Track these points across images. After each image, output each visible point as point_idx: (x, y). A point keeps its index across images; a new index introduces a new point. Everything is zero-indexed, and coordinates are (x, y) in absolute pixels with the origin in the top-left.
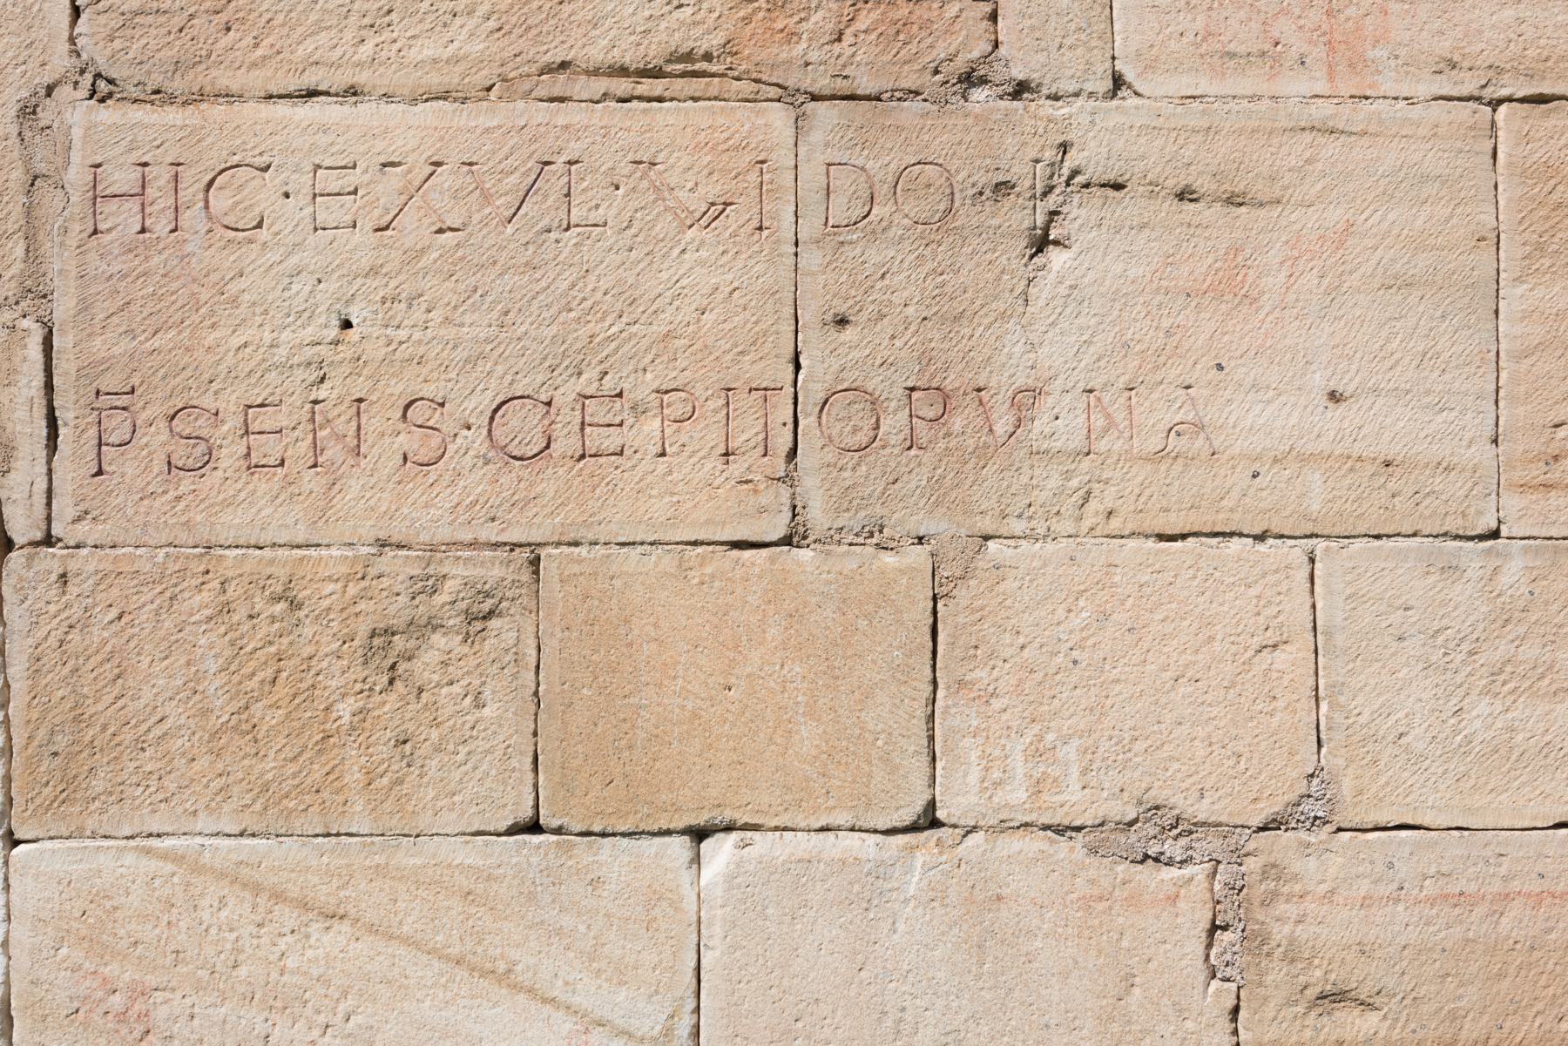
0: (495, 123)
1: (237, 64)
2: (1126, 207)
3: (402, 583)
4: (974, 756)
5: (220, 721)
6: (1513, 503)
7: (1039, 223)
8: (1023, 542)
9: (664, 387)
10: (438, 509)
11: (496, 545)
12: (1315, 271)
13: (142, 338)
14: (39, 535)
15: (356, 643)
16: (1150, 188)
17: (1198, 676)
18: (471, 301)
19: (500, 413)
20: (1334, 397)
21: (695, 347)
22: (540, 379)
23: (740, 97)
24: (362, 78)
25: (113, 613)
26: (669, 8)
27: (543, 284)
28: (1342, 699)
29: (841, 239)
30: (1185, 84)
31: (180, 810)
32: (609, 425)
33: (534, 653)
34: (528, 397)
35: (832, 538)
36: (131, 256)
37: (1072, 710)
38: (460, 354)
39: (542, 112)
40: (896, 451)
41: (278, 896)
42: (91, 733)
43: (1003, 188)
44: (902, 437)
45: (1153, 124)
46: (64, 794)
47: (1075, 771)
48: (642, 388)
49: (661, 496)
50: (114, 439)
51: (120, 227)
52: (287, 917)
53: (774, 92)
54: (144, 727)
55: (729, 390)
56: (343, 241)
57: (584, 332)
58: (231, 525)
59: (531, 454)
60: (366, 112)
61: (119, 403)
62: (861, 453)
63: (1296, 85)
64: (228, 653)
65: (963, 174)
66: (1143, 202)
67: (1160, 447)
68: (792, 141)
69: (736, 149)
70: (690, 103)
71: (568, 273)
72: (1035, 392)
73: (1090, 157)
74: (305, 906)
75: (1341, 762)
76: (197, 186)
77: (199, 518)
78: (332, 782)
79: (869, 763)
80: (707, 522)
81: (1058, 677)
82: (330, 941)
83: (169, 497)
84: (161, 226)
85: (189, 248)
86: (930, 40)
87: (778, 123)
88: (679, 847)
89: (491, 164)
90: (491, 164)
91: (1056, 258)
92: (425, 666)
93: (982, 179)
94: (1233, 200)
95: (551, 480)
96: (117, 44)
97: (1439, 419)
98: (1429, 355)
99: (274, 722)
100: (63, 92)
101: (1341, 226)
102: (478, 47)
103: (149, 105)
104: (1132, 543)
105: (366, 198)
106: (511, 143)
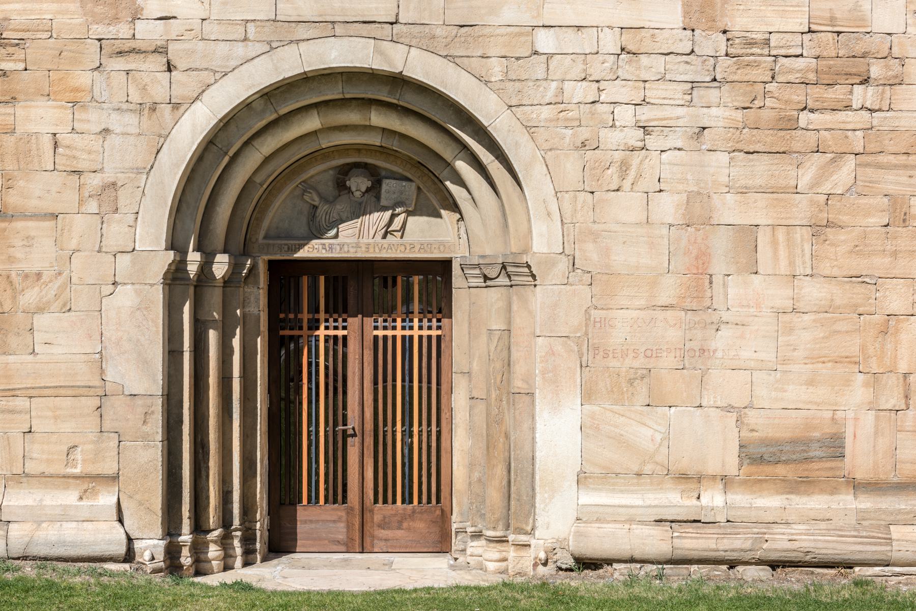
2: (729, 326)
6: (778, 366)
20: (755, 352)
24: (629, 307)
30: (737, 309)
35: (688, 369)
41: (616, 413)
43: (712, 323)
48: (664, 348)
52: (617, 416)
58: (611, 365)
60: (629, 311)
63: (752, 310)
72: (716, 350)
73: (724, 319)
74: (619, 414)
82: (622, 419)
88: (667, 408)
92: (635, 384)
94: (743, 325)
102: (644, 303)
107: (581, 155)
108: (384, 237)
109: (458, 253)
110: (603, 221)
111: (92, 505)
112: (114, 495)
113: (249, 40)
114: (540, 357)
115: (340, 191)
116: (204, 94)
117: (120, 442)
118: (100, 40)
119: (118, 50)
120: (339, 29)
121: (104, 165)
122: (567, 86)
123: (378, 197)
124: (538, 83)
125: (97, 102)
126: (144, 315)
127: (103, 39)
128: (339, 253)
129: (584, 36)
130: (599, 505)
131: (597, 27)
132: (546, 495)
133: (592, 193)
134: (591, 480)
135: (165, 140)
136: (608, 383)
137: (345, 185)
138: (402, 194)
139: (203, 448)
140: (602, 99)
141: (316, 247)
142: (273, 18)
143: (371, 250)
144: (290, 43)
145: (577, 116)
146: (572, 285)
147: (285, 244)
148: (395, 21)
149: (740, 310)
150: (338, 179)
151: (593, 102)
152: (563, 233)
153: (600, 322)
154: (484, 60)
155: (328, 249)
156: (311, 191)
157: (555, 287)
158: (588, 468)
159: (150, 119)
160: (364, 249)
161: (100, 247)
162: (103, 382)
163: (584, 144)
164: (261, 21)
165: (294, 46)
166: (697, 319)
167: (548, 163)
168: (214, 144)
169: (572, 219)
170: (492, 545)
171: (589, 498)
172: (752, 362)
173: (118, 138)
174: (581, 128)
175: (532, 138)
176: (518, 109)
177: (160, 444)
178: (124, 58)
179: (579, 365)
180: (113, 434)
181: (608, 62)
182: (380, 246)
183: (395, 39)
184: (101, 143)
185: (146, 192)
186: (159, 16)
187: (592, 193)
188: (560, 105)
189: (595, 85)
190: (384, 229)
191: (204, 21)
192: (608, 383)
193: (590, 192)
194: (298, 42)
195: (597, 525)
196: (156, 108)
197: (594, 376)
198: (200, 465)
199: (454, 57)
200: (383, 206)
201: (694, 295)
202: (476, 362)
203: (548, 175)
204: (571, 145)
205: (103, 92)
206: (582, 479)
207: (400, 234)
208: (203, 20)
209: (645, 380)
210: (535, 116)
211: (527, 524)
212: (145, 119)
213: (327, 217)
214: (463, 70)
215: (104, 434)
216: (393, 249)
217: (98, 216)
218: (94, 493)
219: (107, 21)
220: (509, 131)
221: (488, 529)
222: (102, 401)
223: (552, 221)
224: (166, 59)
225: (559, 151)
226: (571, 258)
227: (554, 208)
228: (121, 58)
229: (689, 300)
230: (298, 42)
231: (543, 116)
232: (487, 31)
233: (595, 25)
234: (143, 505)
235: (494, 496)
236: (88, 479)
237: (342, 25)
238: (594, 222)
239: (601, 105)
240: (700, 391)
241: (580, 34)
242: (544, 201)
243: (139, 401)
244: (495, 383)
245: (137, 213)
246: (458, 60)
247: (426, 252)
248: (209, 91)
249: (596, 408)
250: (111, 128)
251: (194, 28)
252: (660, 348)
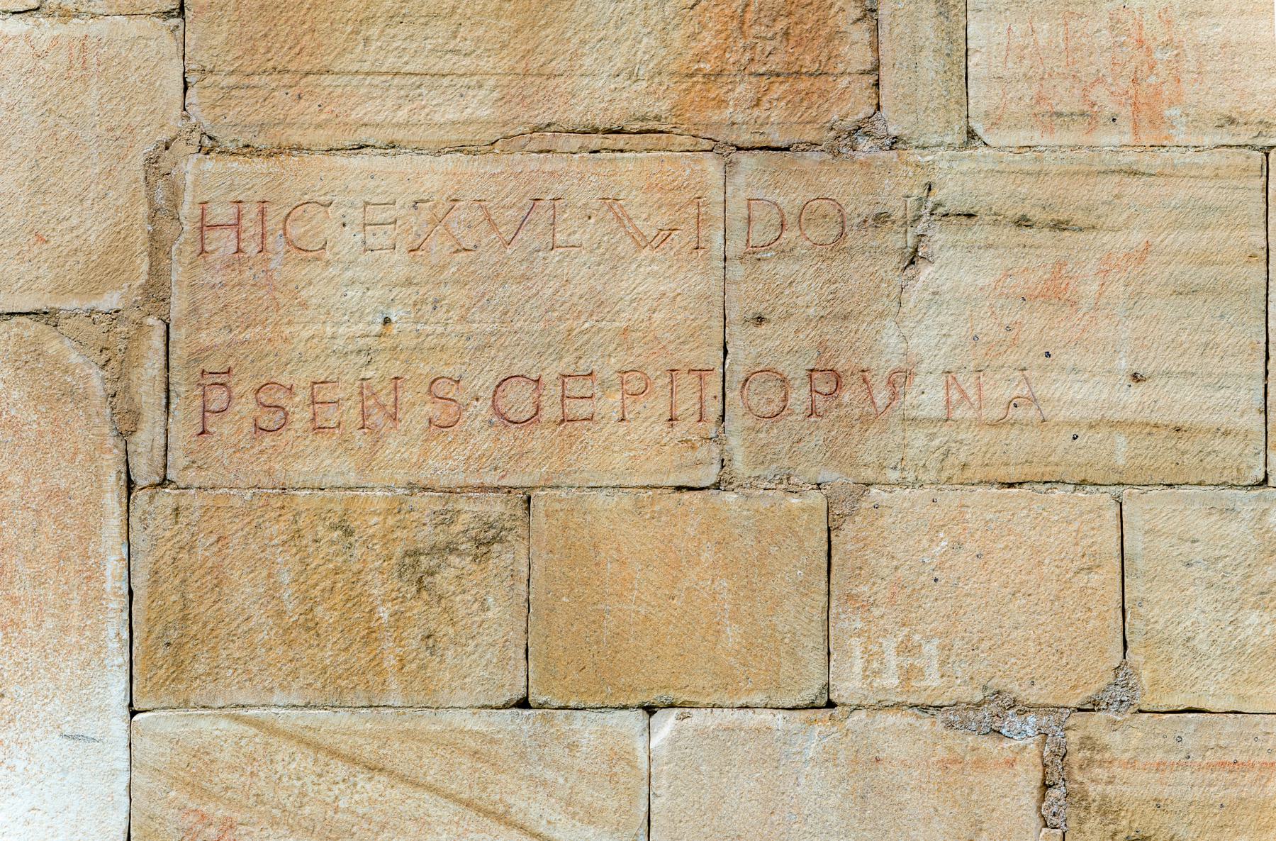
0: (499, 171)
1: (306, 126)
2: (979, 233)
3: (428, 516)
4: (858, 652)
5: (292, 620)
7: (909, 244)
8: (897, 489)
9: (624, 369)
10: (454, 460)
11: (497, 489)
12: (1121, 281)
13: (237, 332)
14: (157, 479)
15: (393, 561)
16: (995, 217)
17: (1030, 592)
18: (480, 304)
19: (501, 388)
20: (1136, 377)
21: (648, 338)
22: (531, 362)
23: (682, 148)
24: (399, 135)
25: (213, 538)
26: (629, 82)
27: (534, 291)
28: (1142, 611)
29: (759, 256)
31: (260, 687)
32: (582, 398)
33: (526, 570)
34: (522, 376)
36: (229, 271)
37: (933, 616)
38: (472, 344)
39: (534, 162)
40: (800, 418)
41: (334, 753)
42: (195, 628)
43: (881, 219)
44: (804, 407)
45: (997, 169)
46: (175, 675)
47: (935, 663)
48: (608, 368)
49: (621, 452)
50: (214, 407)
51: (222, 249)
53: (707, 145)
54: (235, 624)
55: (673, 370)
56: (386, 259)
57: (563, 327)
58: (301, 470)
59: (524, 419)
60: (403, 163)
61: (218, 380)
62: (773, 420)
63: (1108, 138)
64: (299, 568)
65: (852, 207)
66: (988, 228)
67: (1002, 416)
68: (722, 182)
69: (679, 188)
70: (644, 154)
71: (552, 283)
72: (908, 374)
73: (950, 193)
74: (353, 760)
75: (1141, 659)
76: (278, 217)
77: (277, 467)
78: (374, 667)
79: (778, 655)
80: (658, 471)
81: (923, 591)
82: (371, 787)
83: (255, 450)
84: (251, 248)
85: (272, 265)
86: (826, 106)
87: (711, 169)
88: (636, 719)
89: (496, 201)
90: (496, 201)
91: (926, 272)
92: (444, 580)
93: (865, 210)
94: (1059, 226)
95: (539, 439)
96: (218, 111)
97: (1218, 395)
98: (1211, 346)
99: (331, 621)
100: (179, 146)
101: (1142, 247)
102: (484, 113)
103: (241, 158)
104: (980, 490)
105: (403, 227)
106: (511, 185)
136: (286, 578)
149: (1038, 138)
153: (237, 225)
166: (792, 197)
172: (1121, 441)
197: (204, 541)
201: (775, 63)
209: (502, 557)
229: (743, 89)
240: (818, 616)
249: (212, 727)
252: (583, 366)
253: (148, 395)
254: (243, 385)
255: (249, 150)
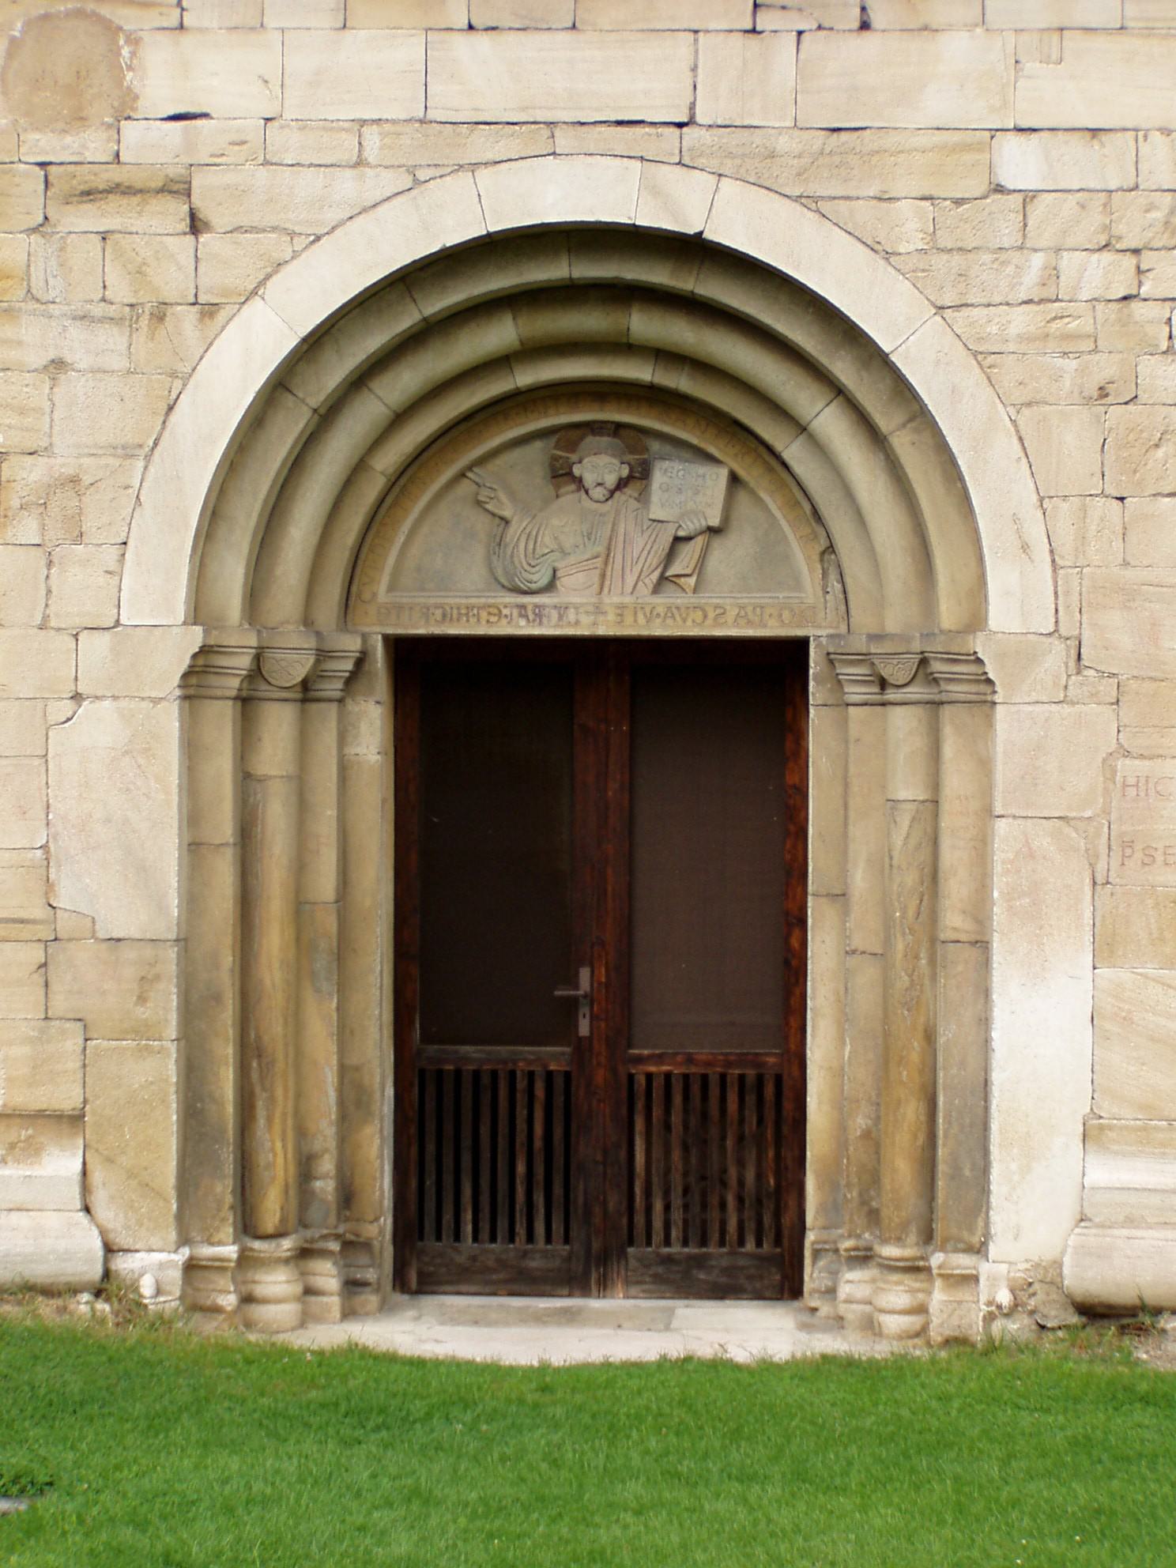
84: (1142, 794)
107: (1098, 417)
108: (657, 589)
109: (819, 633)
110: (1145, 563)
111: (30, 1176)
112: (74, 1155)
113: (368, 165)
114: (1003, 862)
115: (557, 487)
116: (269, 284)
117: (86, 1040)
118: (42, 165)
119: (82, 187)
120: (564, 140)
121: (56, 440)
122: (1069, 262)
123: (643, 498)
124: (1003, 256)
125: (38, 300)
126: (139, 766)
127: (50, 163)
128: (556, 626)
129: (1106, 151)
130: (1129, 1189)
131: (1136, 130)
132: (1014, 1166)
133: (1122, 499)
134: (1110, 1134)
135: (185, 385)
136: (1153, 921)
137: (570, 474)
138: (697, 492)
139: (260, 1056)
140: (1145, 291)
141: (505, 611)
142: (421, 114)
143: (629, 619)
144: (457, 170)
145: (1089, 329)
146: (1073, 703)
147: (437, 607)
148: (686, 120)
150: (555, 458)
151: (1125, 298)
152: (1056, 587)
153: (1137, 785)
154: (884, 205)
155: (531, 617)
156: (495, 486)
157: (1038, 708)
158: (1107, 1108)
159: (152, 339)
160: (611, 617)
161: (46, 618)
162: (52, 912)
163: (1103, 392)
164: (394, 122)
165: (465, 177)
167: (1023, 433)
168: (290, 391)
169: (1077, 557)
170: (895, 1277)
171: (1105, 1172)
173: (83, 379)
174: (1097, 357)
175: (989, 378)
176: (956, 314)
177: (173, 1048)
178: (98, 204)
179: (1088, 881)
180: (68, 1025)
181: (1157, 208)
182: (648, 610)
183: (686, 161)
184: (47, 391)
185: (142, 498)
186: (171, 113)
187: (1122, 499)
188: (1049, 305)
189: (1130, 261)
190: (659, 570)
191: (269, 124)
192: (1153, 921)
193: (1117, 498)
194: (474, 167)
195: (1125, 1232)
196: (165, 315)
198: (252, 1094)
199: (816, 199)
200: (654, 521)
202: (860, 871)
203: (1024, 460)
204: (1076, 394)
205: (51, 281)
206: (1092, 1134)
207: (692, 581)
208: (268, 120)
210: (994, 329)
211: (971, 1230)
212: (141, 338)
213: (531, 546)
214: (837, 228)
215: (53, 1023)
216: (678, 618)
217: (40, 549)
218: (31, 1151)
219: (61, 125)
220: (938, 362)
221: (885, 1241)
222: (50, 951)
223: (1032, 561)
224: (186, 208)
225: (1048, 408)
226: (1074, 643)
227: (1036, 533)
228: (89, 206)
230: (474, 167)
231: (1013, 330)
232: (890, 141)
233: (1130, 126)
234: (136, 1177)
235: (901, 1170)
236: (18, 1121)
237: (571, 127)
238: (1126, 564)
239: (1142, 304)
241: (1097, 147)
242: (1015, 519)
243: (129, 953)
244: (903, 917)
245: (125, 543)
246: (825, 207)
247: (750, 623)
248: (279, 275)
249: (1124, 975)
250: (69, 359)
251: (248, 138)
253: (1103, 850)
254: (1139, 846)
255: (1142, 757)
